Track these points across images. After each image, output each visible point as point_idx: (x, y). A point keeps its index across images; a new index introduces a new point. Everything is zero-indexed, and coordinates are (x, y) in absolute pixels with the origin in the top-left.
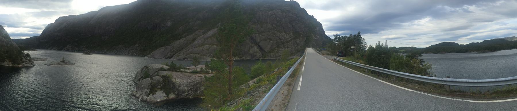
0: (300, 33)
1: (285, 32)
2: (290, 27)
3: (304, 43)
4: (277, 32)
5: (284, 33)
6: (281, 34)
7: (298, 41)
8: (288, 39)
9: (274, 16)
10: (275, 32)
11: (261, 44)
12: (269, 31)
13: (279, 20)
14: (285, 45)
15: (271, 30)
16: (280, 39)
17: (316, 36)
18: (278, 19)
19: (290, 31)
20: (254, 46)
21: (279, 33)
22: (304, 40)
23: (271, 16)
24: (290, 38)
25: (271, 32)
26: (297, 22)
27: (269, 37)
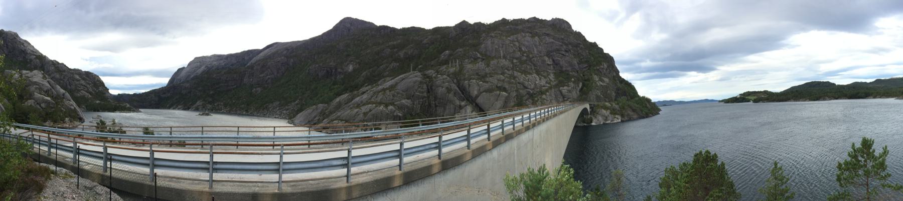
0: (571, 73)
1: (538, 73)
2: (549, 63)
3: (578, 93)
4: (519, 74)
5: (535, 75)
6: (527, 78)
7: (565, 90)
8: (544, 86)
9: (517, 44)
10: (516, 73)
11: (480, 100)
12: (503, 74)
13: (526, 50)
14: (536, 99)
15: (508, 70)
16: (527, 88)
17: (603, 78)
18: (523, 49)
19: (549, 71)
20: (466, 106)
21: (523, 75)
22: (578, 86)
23: (511, 43)
24: (547, 85)
25: (506, 75)
26: (564, 53)
27: (499, 85)
